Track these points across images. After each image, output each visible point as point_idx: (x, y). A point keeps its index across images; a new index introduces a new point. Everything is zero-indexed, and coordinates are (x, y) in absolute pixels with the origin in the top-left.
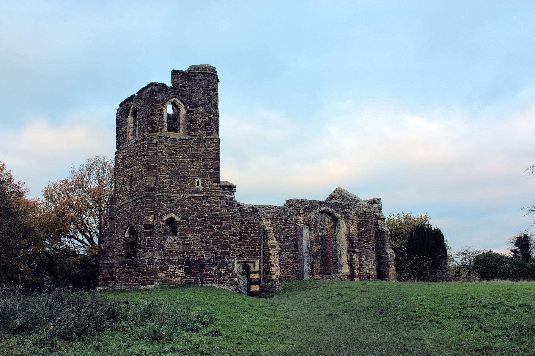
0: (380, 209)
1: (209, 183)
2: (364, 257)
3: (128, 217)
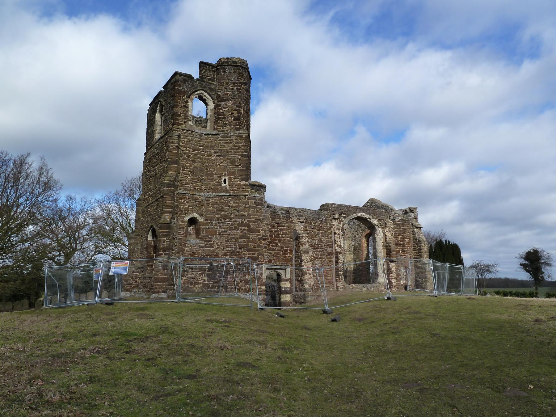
0: (416, 218)
1: (237, 181)
2: (401, 267)
3: (150, 218)
